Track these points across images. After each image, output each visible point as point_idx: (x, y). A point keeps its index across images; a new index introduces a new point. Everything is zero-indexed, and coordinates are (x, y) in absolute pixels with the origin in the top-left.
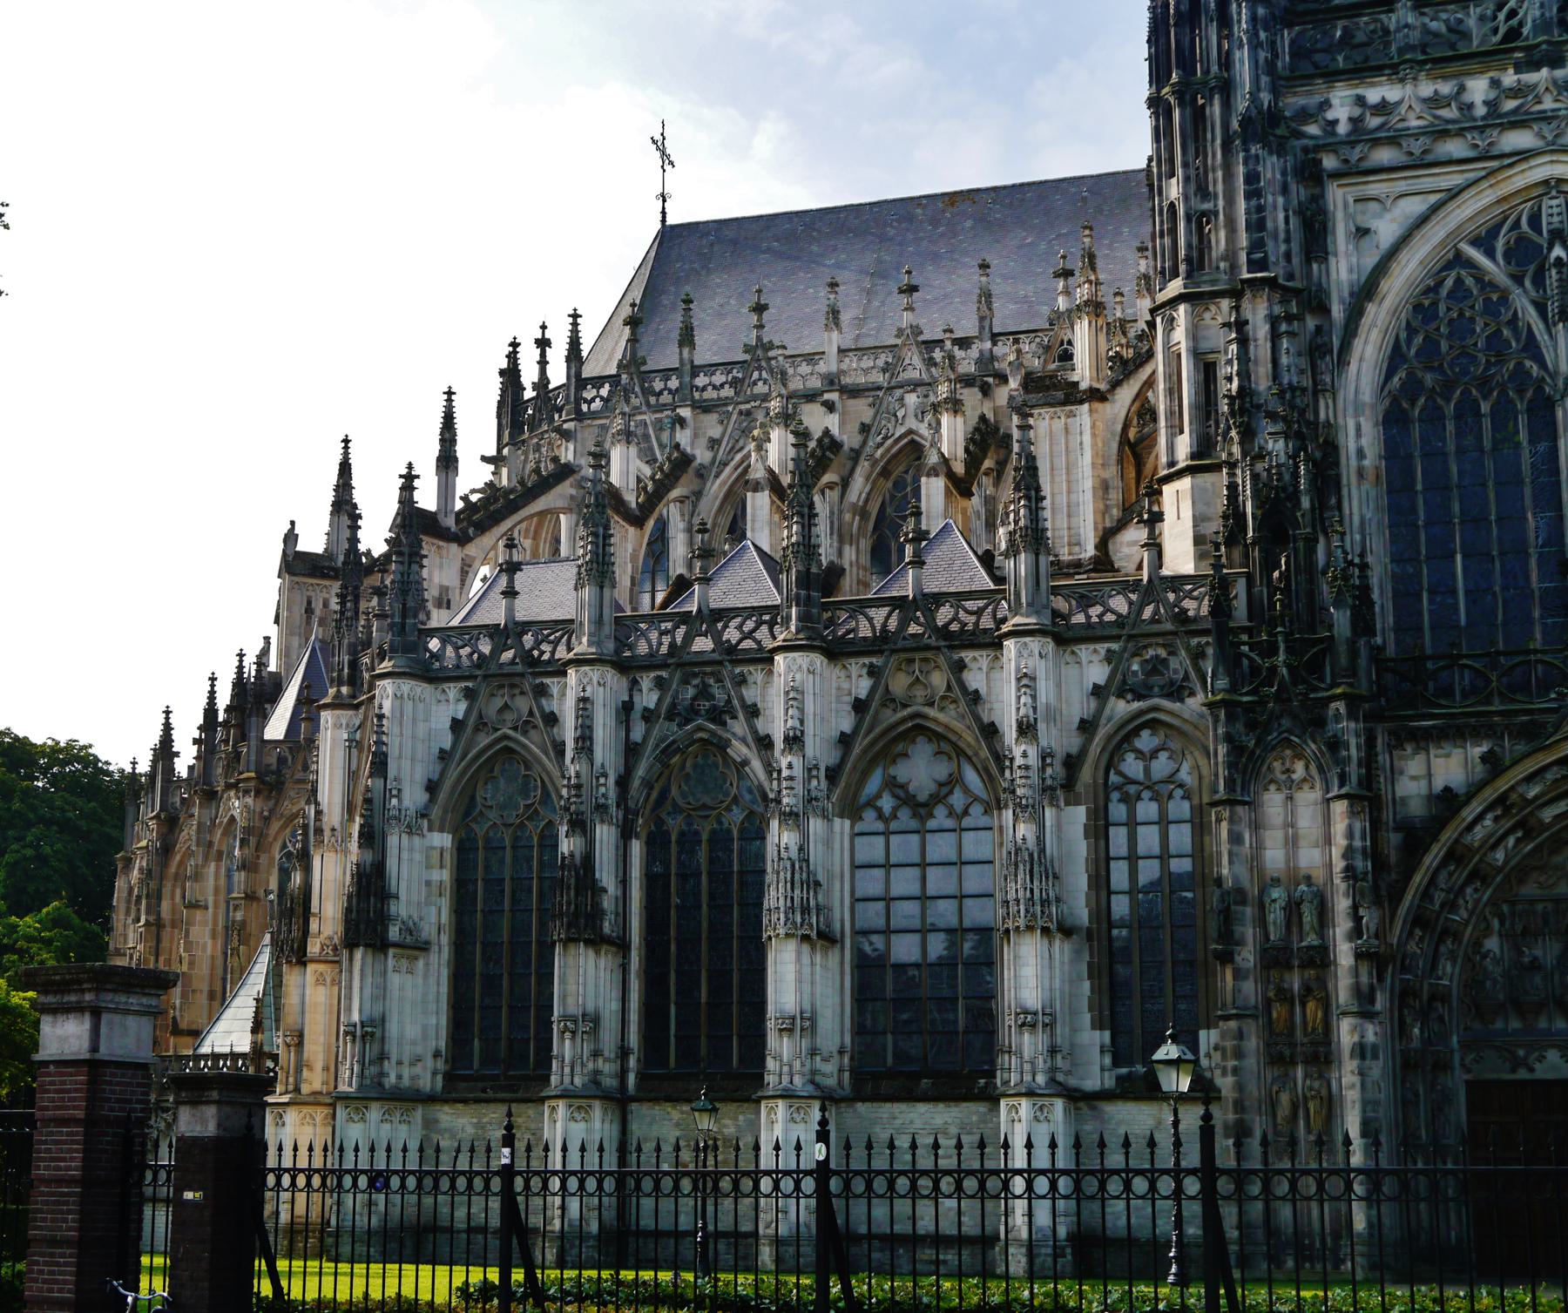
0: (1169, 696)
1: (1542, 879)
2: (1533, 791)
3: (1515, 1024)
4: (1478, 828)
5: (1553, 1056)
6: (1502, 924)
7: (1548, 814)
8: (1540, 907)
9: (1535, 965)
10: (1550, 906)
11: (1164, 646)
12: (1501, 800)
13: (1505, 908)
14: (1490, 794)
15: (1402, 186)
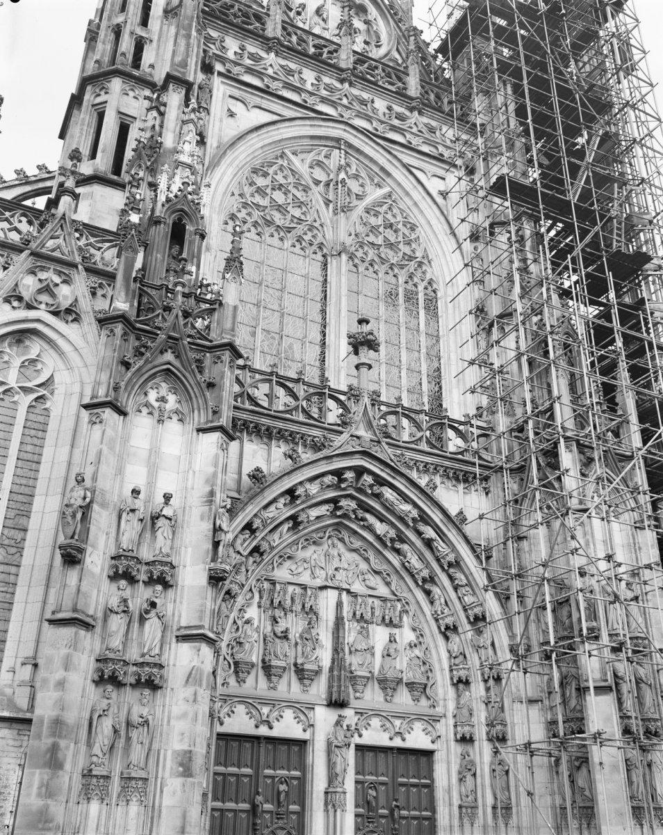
0: (56, 313)
1: (293, 568)
2: (313, 488)
3: (263, 682)
4: (272, 508)
5: (289, 714)
6: (261, 597)
7: (314, 513)
8: (291, 589)
9: (285, 636)
10: (298, 590)
11: (59, 273)
12: (291, 492)
13: (266, 585)
14: (287, 484)
15: (258, 101)
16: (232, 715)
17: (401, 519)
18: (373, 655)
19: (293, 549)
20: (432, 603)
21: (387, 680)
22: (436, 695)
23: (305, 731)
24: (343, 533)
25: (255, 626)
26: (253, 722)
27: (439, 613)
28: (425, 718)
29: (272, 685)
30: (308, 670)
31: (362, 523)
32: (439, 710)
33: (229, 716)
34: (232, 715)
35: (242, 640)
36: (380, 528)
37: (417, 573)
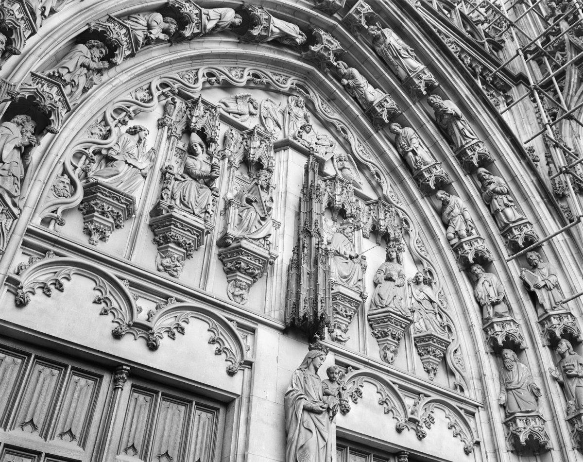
16: (54, 292)
17: (407, 84)
18: (364, 268)
19: (234, 72)
20: (446, 226)
21: (389, 319)
22: (464, 369)
23: (231, 373)
24: (312, 94)
25: (148, 148)
26: (108, 324)
27: (464, 233)
28: (454, 404)
29: (167, 262)
30: (249, 252)
31: (345, 81)
32: (472, 394)
33: (47, 292)
34: (54, 292)
35: (112, 153)
36: (374, 95)
37: (429, 171)
